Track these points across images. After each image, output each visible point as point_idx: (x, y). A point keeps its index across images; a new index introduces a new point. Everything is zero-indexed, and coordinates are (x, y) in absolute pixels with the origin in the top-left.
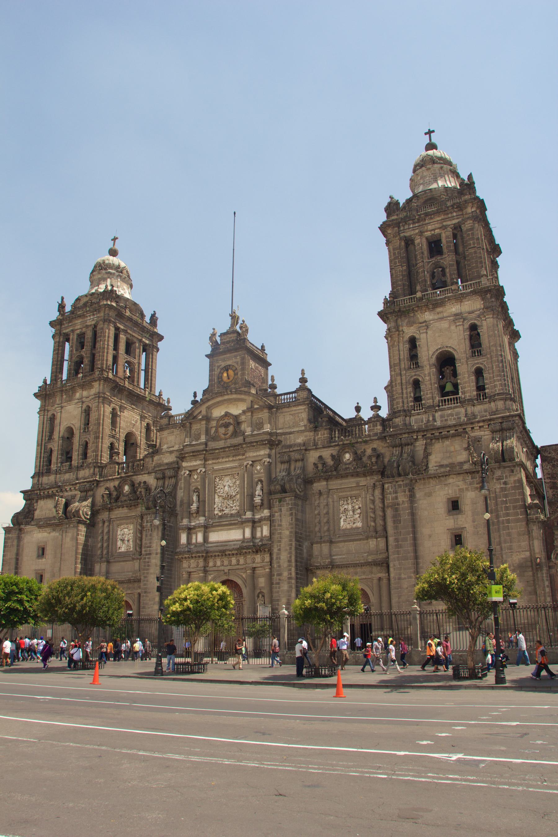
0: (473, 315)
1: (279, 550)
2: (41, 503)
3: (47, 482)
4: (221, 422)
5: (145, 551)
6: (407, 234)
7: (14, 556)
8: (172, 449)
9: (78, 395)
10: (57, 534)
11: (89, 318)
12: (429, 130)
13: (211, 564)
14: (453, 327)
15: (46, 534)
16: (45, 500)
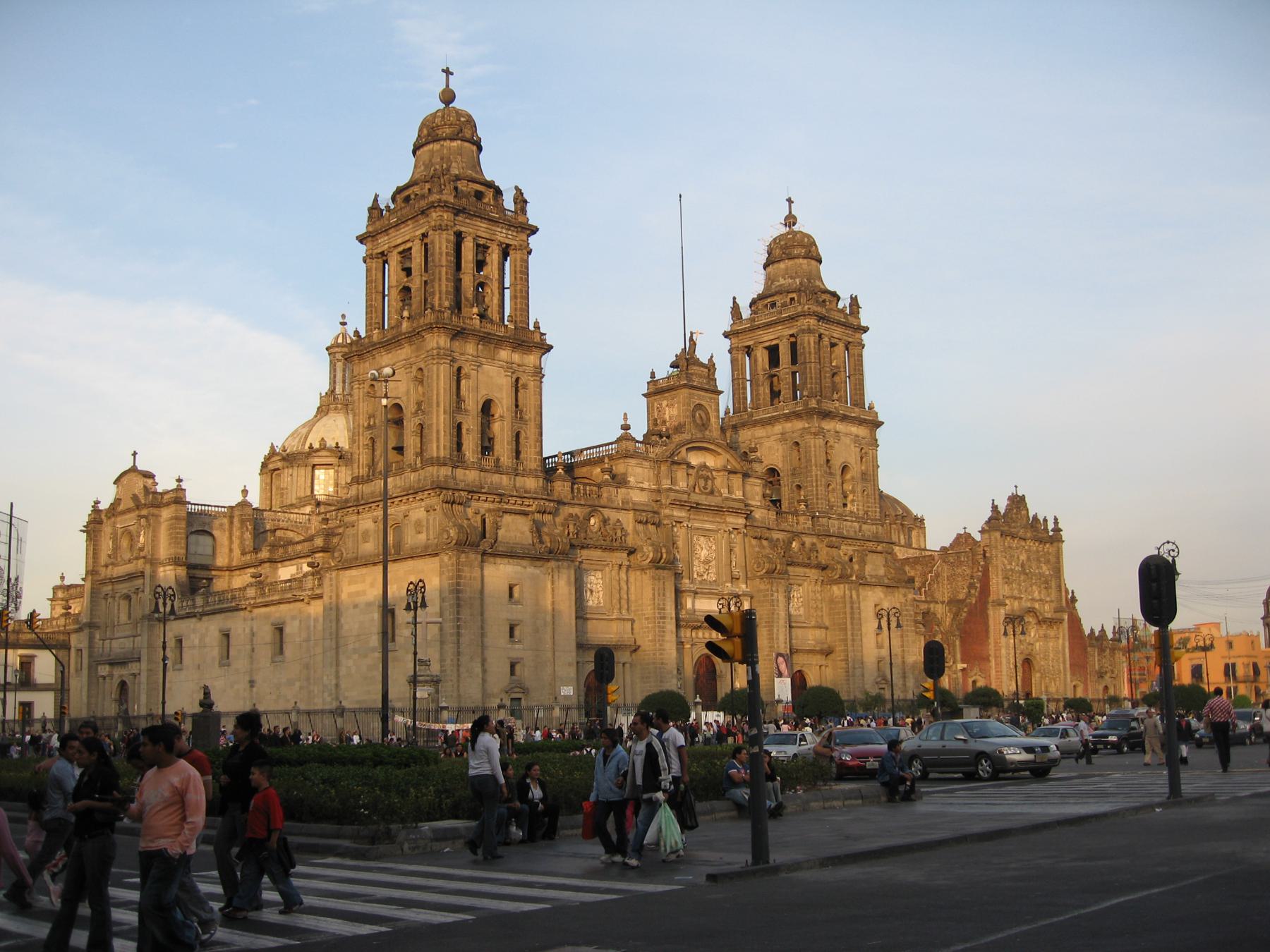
0: (863, 441)
1: (778, 630)
2: (508, 518)
3: (462, 478)
4: (701, 473)
5: (659, 613)
6: (822, 331)
7: (478, 596)
8: (641, 485)
9: (504, 354)
10: (537, 571)
11: (499, 230)
12: (790, 198)
13: (694, 634)
14: (852, 446)
15: (519, 568)
16: (513, 516)
